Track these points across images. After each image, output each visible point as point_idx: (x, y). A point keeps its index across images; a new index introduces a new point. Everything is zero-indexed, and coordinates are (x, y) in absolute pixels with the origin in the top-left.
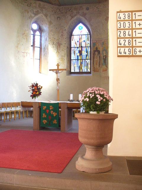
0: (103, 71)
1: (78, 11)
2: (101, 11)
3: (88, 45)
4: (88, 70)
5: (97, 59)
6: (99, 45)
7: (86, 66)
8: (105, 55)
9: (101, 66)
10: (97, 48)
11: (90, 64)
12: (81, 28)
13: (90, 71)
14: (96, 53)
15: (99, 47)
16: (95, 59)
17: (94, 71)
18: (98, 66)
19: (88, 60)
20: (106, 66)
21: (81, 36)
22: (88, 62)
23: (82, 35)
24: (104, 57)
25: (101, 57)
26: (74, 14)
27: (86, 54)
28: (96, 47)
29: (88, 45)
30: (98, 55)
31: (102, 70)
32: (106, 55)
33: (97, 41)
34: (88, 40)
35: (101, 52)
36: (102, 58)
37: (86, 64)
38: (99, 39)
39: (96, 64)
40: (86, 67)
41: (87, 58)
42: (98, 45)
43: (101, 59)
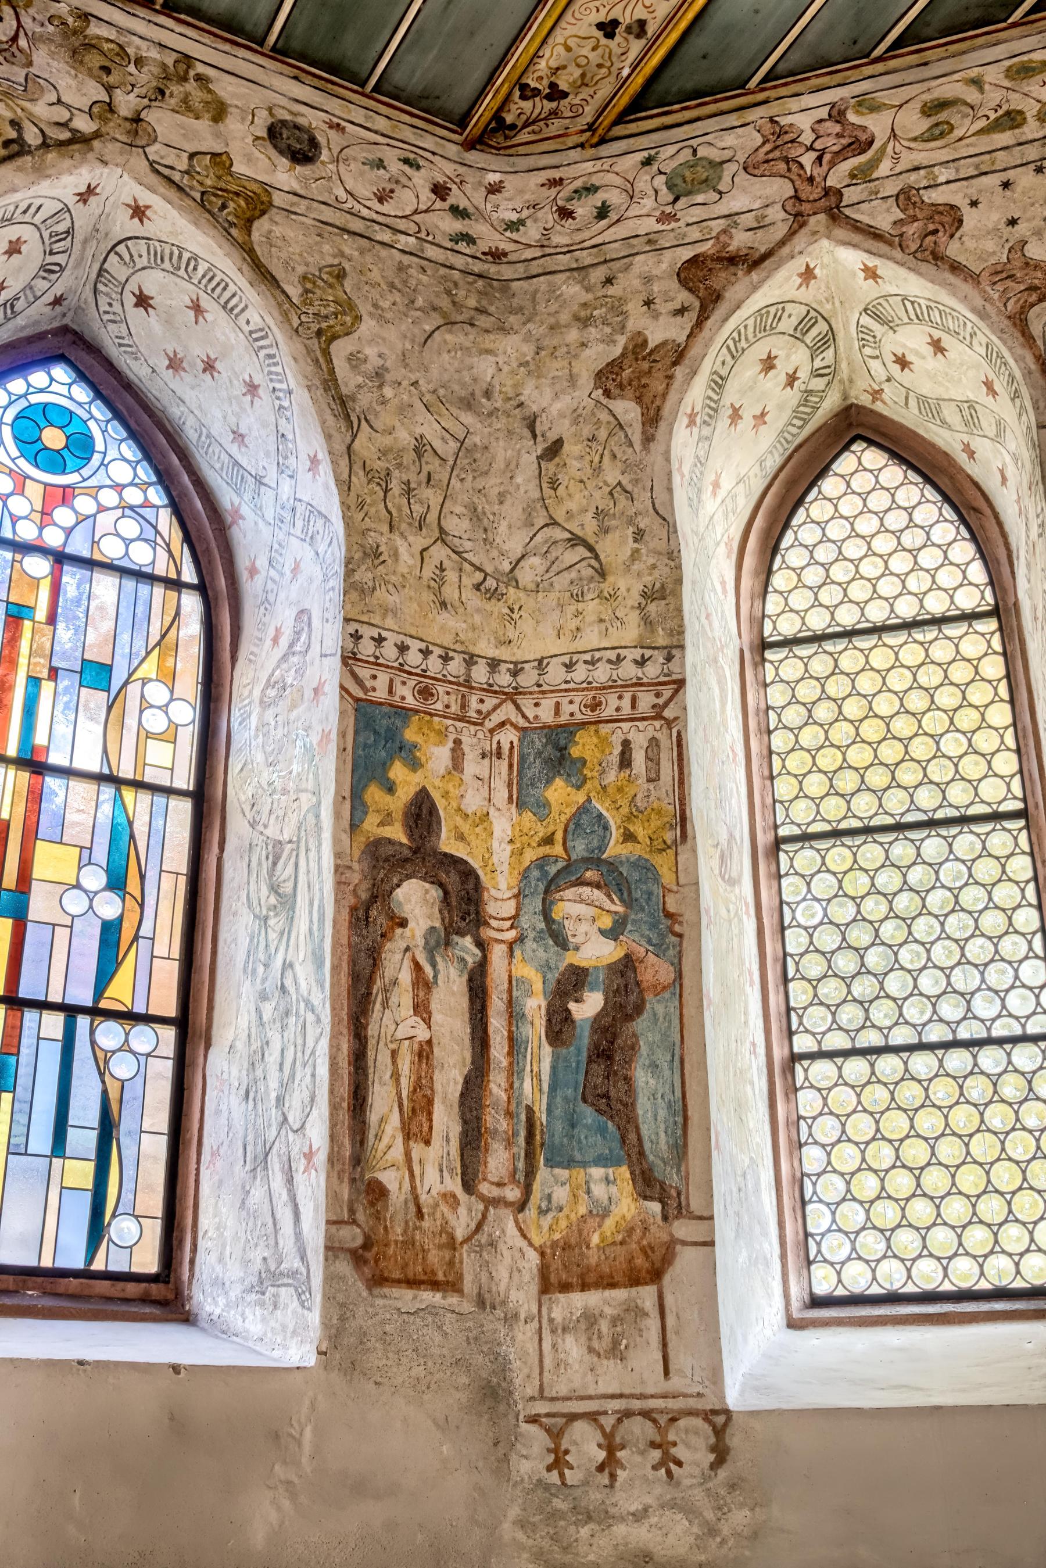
0: (549, 1284)
1: (126, 103)
2: (497, 256)
3: (158, 753)
4: (122, 1229)
5: (426, 1022)
6: (473, 766)
7: (83, 1139)
8: (596, 951)
9: (498, 1161)
10: (422, 814)
11: (158, 1117)
12: (53, 438)
13: (148, 1262)
14: (416, 900)
15: (473, 802)
16: (395, 1021)
17: (358, 1257)
18: (435, 1169)
19: (143, 1038)
20: (647, 1183)
21: (38, 566)
22: (122, 1068)
23: (60, 558)
24: (589, 1006)
25: (496, 1004)
26: (41, 109)
27: (109, 907)
28: (406, 781)
29: (158, 753)
30: (440, 941)
31: (512, 1265)
32: (627, 965)
33: (425, 693)
34: (169, 678)
35: (499, 898)
36: (535, 1005)
37: (85, 1110)
38: (471, 660)
39: (416, 1123)
40: (80, 1173)
41: (121, 992)
42: (438, 756)
43: (497, 1025)
